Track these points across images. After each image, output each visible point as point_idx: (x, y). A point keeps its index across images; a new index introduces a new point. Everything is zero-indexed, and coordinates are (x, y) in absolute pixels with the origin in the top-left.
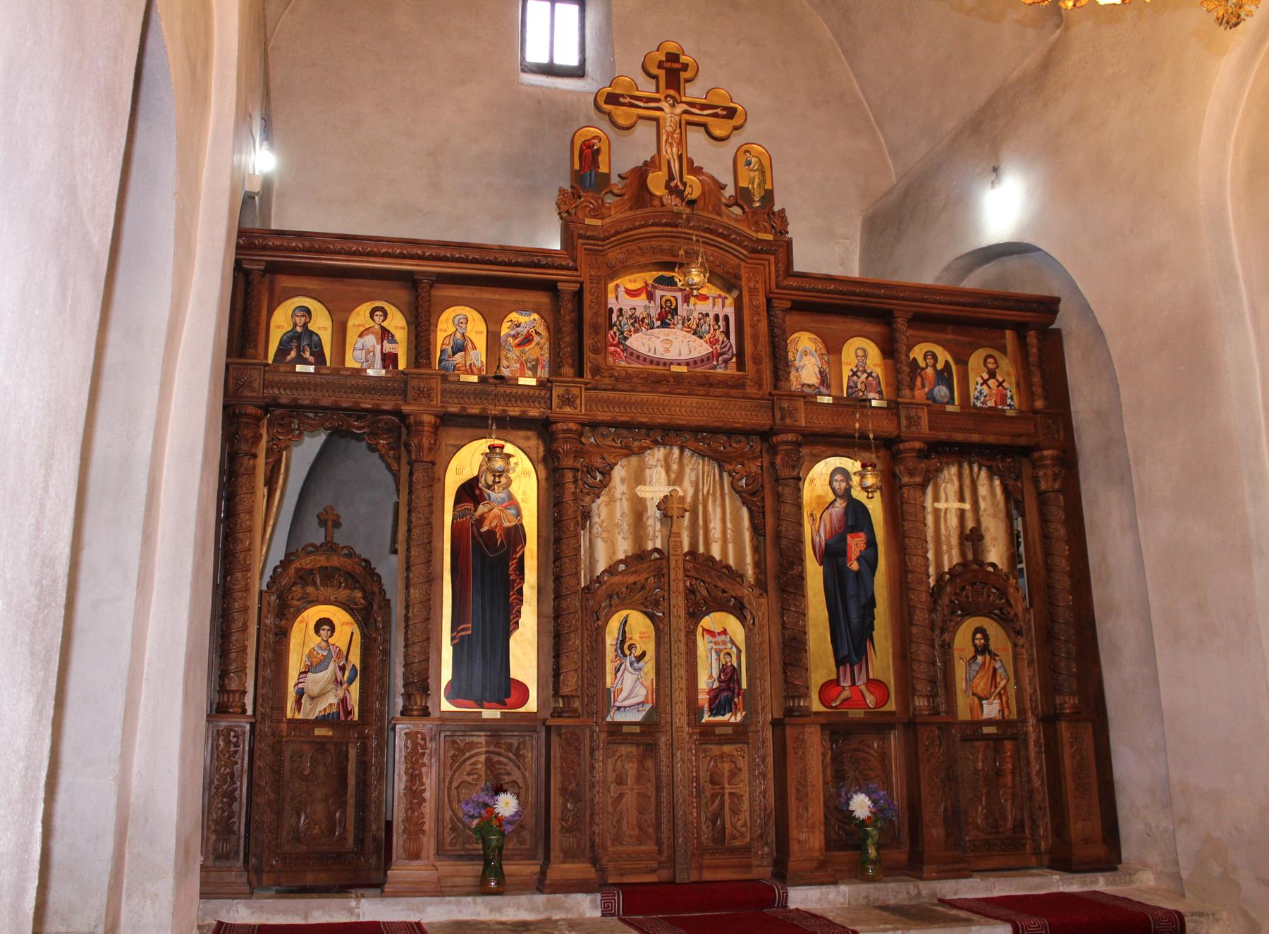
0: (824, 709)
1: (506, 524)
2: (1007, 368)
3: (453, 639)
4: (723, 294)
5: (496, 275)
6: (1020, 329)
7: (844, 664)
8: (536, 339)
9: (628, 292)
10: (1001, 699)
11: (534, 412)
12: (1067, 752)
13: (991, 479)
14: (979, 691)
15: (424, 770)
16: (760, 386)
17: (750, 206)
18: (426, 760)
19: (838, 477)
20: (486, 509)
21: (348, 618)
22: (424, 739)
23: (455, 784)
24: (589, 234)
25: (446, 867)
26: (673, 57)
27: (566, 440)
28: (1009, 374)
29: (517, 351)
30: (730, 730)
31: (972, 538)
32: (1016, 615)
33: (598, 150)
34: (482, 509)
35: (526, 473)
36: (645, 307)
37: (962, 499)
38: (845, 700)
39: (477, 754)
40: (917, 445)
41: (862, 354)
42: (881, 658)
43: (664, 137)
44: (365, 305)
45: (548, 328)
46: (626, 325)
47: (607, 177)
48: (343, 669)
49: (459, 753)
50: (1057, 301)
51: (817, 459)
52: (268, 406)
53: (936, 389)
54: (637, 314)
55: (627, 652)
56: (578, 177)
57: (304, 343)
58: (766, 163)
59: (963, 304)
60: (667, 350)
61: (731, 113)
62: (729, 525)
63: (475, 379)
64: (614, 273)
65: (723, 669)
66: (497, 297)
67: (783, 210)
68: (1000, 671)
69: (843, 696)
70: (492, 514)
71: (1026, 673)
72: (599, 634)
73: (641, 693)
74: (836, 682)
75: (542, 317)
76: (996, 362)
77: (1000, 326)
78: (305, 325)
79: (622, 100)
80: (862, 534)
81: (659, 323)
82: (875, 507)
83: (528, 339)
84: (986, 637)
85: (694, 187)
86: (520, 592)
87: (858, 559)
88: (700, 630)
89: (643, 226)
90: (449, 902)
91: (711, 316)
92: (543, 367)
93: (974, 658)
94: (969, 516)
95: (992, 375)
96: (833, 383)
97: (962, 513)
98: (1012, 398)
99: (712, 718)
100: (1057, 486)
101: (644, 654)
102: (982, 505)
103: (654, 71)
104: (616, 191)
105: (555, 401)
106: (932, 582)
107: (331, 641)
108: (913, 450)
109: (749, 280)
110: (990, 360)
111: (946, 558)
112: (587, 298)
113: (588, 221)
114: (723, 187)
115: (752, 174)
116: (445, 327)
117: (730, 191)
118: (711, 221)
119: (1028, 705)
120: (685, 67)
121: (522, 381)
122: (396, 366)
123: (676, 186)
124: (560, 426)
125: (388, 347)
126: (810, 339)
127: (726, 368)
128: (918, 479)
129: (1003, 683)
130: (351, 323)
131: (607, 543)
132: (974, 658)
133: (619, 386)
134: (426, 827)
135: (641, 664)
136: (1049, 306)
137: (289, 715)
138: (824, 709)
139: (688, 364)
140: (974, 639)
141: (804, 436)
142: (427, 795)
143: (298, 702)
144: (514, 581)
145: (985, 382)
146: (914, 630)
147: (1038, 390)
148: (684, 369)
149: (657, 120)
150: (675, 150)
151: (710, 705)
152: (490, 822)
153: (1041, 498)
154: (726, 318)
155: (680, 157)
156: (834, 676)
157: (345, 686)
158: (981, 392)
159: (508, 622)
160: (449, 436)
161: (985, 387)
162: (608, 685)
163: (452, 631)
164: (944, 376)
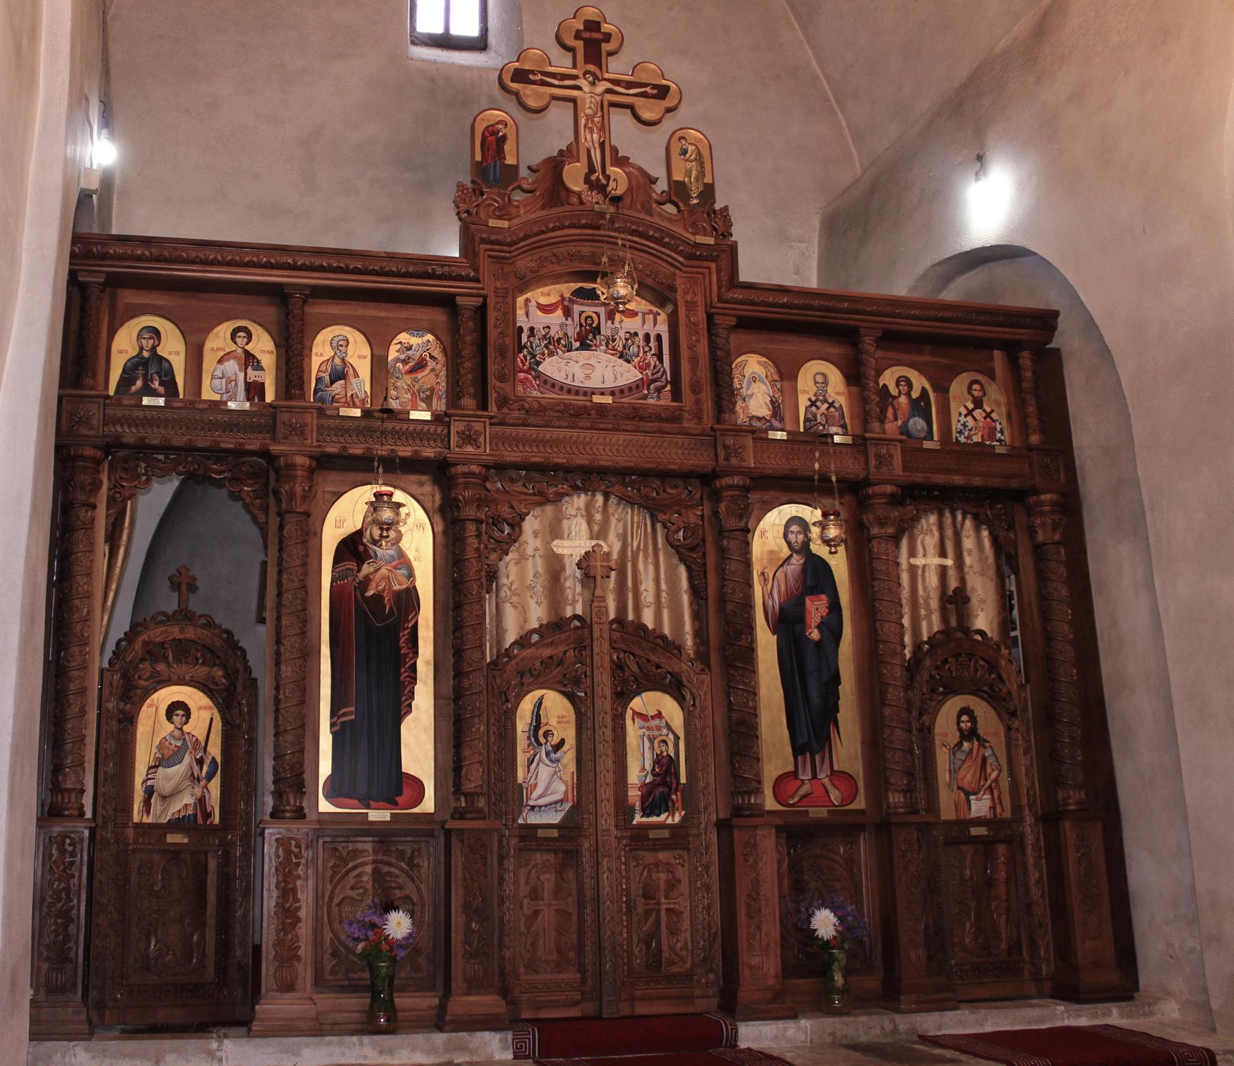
0: (779, 807)
1: (397, 587)
2: (996, 397)
3: (332, 725)
4: (655, 309)
5: (381, 288)
6: (1011, 349)
7: (803, 753)
8: (431, 364)
9: (541, 308)
10: (992, 794)
11: (428, 453)
12: (1072, 857)
13: (977, 530)
14: (966, 785)
15: (299, 883)
16: (700, 419)
17: (687, 204)
18: (301, 870)
19: (794, 528)
20: (372, 569)
21: (206, 701)
22: (298, 846)
23: (336, 900)
24: (493, 238)
25: (327, 1001)
26: (593, 26)
27: (467, 486)
28: (998, 404)
29: (408, 379)
30: (666, 834)
31: (956, 601)
32: (1009, 693)
33: (504, 138)
34: (366, 569)
35: (420, 526)
36: (561, 325)
37: (943, 554)
39: (363, 864)
40: (889, 489)
41: (821, 380)
43: (583, 122)
44: (226, 325)
45: (444, 351)
46: (539, 346)
47: (515, 168)
48: (200, 762)
49: (341, 863)
50: (1055, 315)
51: (768, 507)
52: (110, 447)
53: (911, 421)
54: (552, 333)
55: (542, 740)
56: (480, 171)
57: (152, 370)
58: (705, 153)
59: (943, 320)
60: (588, 377)
61: (663, 92)
62: (664, 586)
63: (357, 413)
64: (524, 285)
65: (658, 760)
66: (382, 314)
67: (726, 208)
68: (990, 760)
69: (803, 791)
70: (379, 574)
71: (1022, 761)
72: (509, 717)
73: (559, 790)
74: (794, 774)
75: (437, 338)
76: (983, 389)
77: (987, 345)
79: (531, 77)
80: (823, 596)
81: (577, 344)
82: (839, 564)
83: (420, 365)
84: (973, 719)
85: (619, 181)
86: (413, 668)
87: (818, 627)
88: (629, 713)
89: (559, 228)
90: (329, 1043)
91: (641, 335)
92: (439, 398)
93: (960, 744)
94: (952, 573)
95: (978, 404)
96: (788, 416)
97: (943, 570)
98: (1002, 432)
99: (644, 819)
100: (1057, 537)
101: (562, 742)
102: (968, 560)
103: (570, 42)
104: (525, 186)
105: (454, 439)
106: (908, 653)
107: (186, 728)
108: (884, 494)
109: (686, 292)
110: (976, 387)
111: (924, 624)
112: (492, 315)
113: (493, 223)
114: (654, 181)
115: (689, 165)
116: (321, 351)
117: (662, 186)
118: (640, 222)
119: (1025, 801)
120: (608, 37)
121: (414, 415)
122: (262, 398)
123: (598, 179)
124: (460, 469)
125: (253, 375)
126: (759, 362)
127: (659, 398)
128: (891, 530)
129: (994, 774)
131: (519, 609)
132: (960, 744)
133: (531, 420)
134: (301, 953)
135: (559, 754)
136: (1046, 321)
138: (779, 807)
139: (612, 393)
140: (958, 722)
141: (752, 479)
142: (302, 913)
143: (147, 803)
144: (406, 655)
145: (970, 413)
146: (887, 711)
147: (1033, 422)
148: (608, 400)
149: (573, 100)
150: (595, 136)
151: (643, 803)
152: (380, 947)
153: (1039, 552)
154: (659, 338)
155: (602, 145)
156: (791, 768)
157: (203, 783)
158: (964, 425)
159: (400, 706)
160: (328, 481)
161: (969, 418)
162: (520, 780)
163: (332, 717)
164: (920, 406)
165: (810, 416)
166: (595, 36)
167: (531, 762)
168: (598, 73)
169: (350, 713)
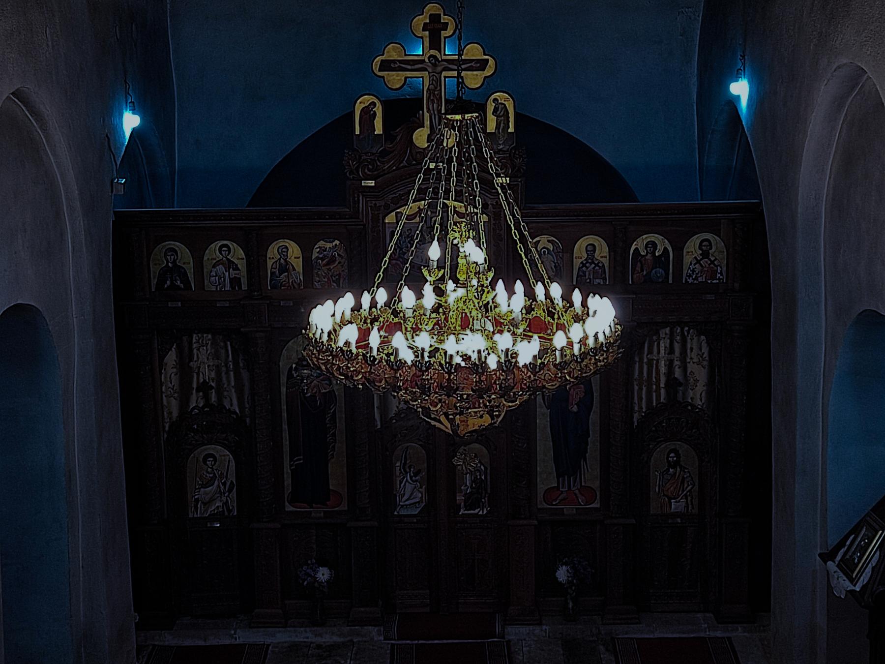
3: (291, 466)
8: (338, 259)
10: (687, 498)
13: (699, 335)
37: (671, 351)
38: (561, 500)
42: (591, 473)
48: (224, 484)
74: (558, 488)
78: (174, 262)
84: (678, 455)
86: (334, 435)
122: (240, 287)
126: (549, 241)
129: (689, 488)
130: (205, 258)
137: (191, 516)
145: (698, 262)
164: (661, 261)
165: (581, 273)
166: (437, 26)
167: (401, 483)
168: (439, 57)
169: (300, 460)
